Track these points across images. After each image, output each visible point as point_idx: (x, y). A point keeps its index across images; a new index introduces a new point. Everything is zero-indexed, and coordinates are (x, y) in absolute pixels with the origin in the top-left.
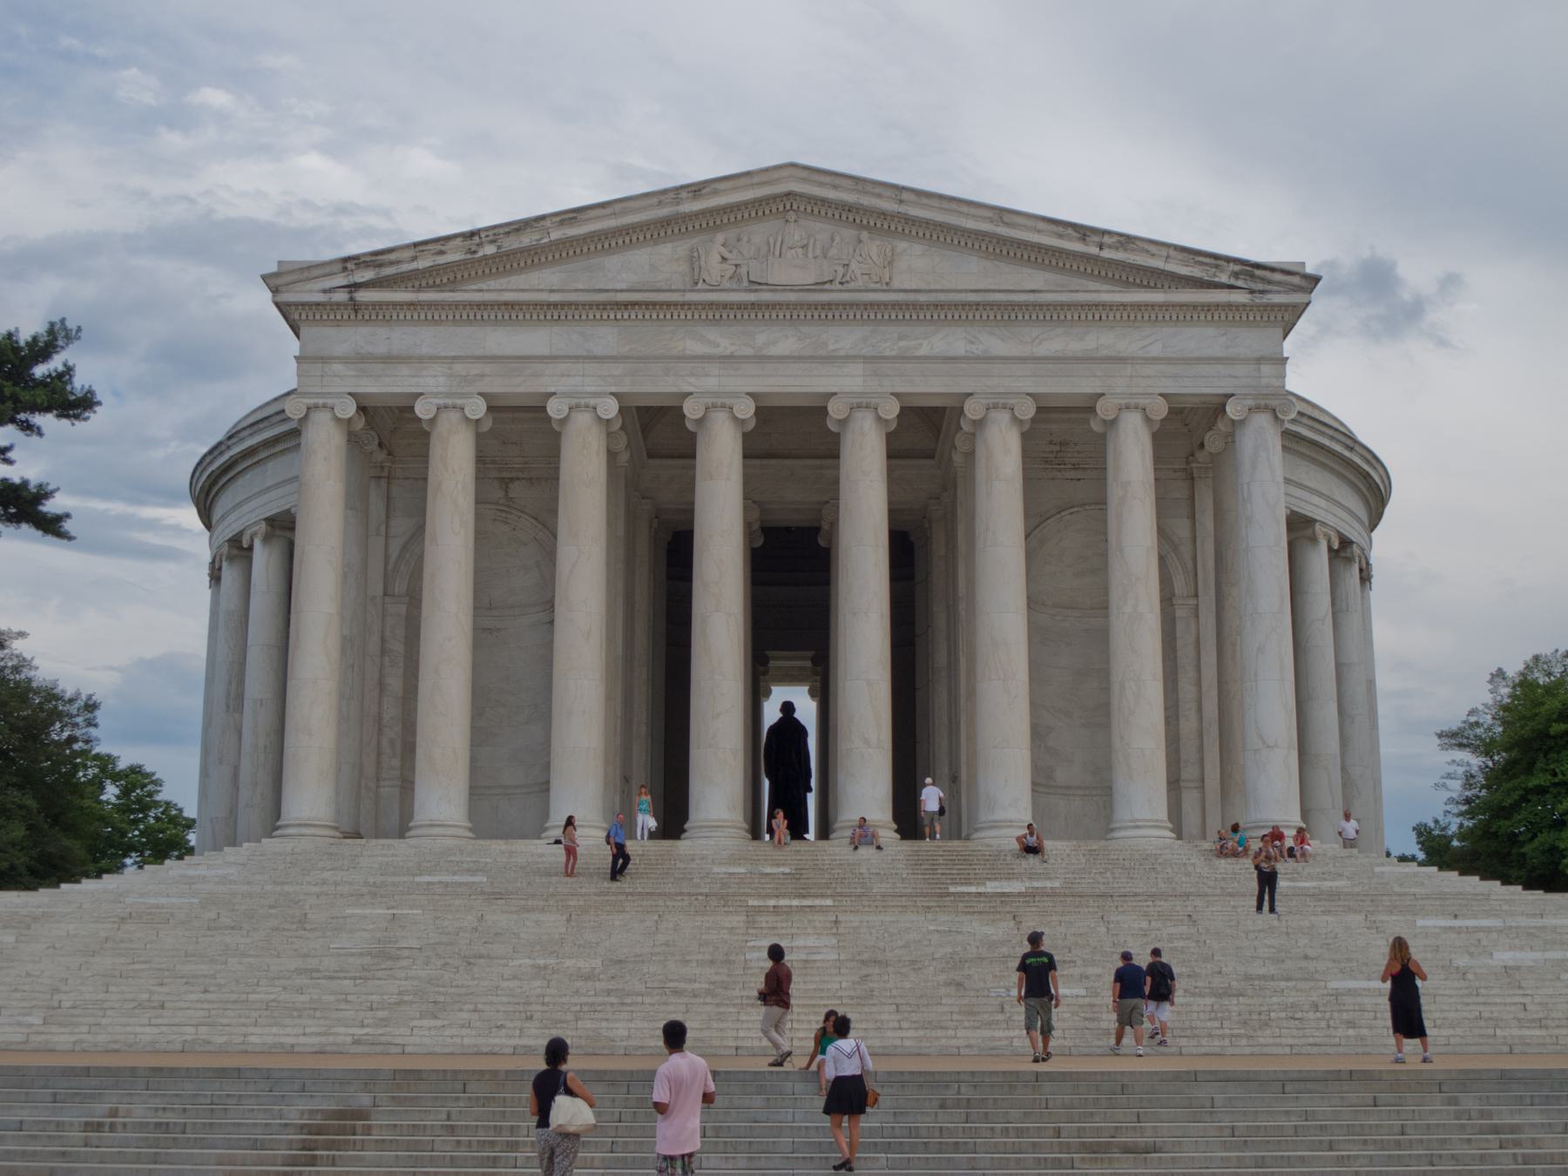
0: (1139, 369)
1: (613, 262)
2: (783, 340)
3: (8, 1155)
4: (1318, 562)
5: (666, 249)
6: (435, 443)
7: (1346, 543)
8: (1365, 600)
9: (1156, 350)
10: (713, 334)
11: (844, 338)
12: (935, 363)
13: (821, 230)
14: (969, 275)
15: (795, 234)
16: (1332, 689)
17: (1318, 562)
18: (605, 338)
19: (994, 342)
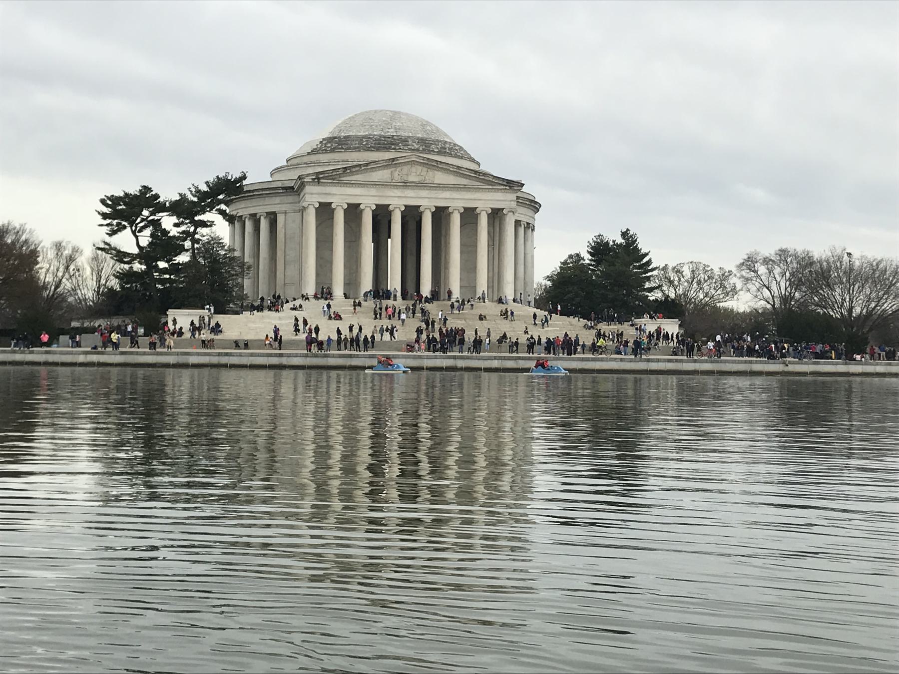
0: (485, 201)
1: (374, 174)
2: (410, 193)
3: (4, 363)
4: (521, 230)
5: (385, 171)
6: (335, 212)
7: (528, 224)
8: (533, 238)
9: (490, 198)
10: (396, 191)
11: (424, 193)
12: (442, 199)
13: (419, 168)
14: (451, 180)
15: (414, 169)
16: (524, 263)
17: (521, 230)
18: (373, 191)
19: (455, 195)
